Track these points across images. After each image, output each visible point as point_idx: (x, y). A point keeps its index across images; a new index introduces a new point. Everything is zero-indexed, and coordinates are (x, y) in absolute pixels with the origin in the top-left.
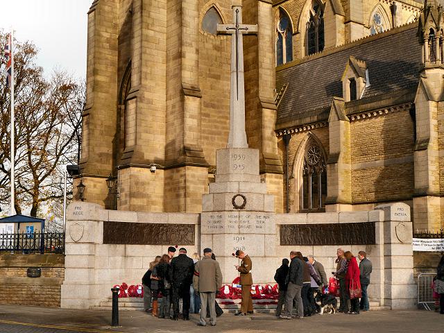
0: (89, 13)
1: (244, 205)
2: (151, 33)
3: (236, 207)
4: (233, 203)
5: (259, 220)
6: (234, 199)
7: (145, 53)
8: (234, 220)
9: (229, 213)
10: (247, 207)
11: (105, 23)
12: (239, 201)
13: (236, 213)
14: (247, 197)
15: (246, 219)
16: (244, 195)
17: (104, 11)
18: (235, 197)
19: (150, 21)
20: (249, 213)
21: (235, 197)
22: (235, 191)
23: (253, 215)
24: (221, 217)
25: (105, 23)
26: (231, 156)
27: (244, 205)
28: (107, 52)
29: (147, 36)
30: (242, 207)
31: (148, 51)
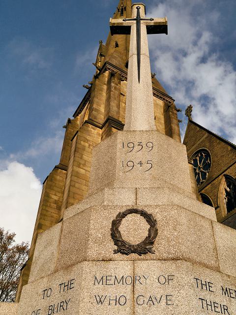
0: (44, 184)
1: (150, 241)
2: (82, 171)
3: (123, 248)
4: (115, 234)
5: (209, 297)
6: (116, 224)
7: (74, 186)
8: (112, 292)
9: (98, 270)
10: (160, 246)
11: (55, 188)
12: (134, 230)
13: (123, 266)
14: (158, 217)
15: (158, 291)
16: (149, 211)
17: (56, 179)
18: (122, 216)
19: (82, 162)
20: (171, 267)
21: (122, 216)
22: (126, 200)
23: (184, 275)
24: (71, 282)
25: (55, 188)
26: (119, 146)
27: (150, 241)
28: (53, 211)
29: (77, 172)
30: (144, 248)
31: (77, 185)
